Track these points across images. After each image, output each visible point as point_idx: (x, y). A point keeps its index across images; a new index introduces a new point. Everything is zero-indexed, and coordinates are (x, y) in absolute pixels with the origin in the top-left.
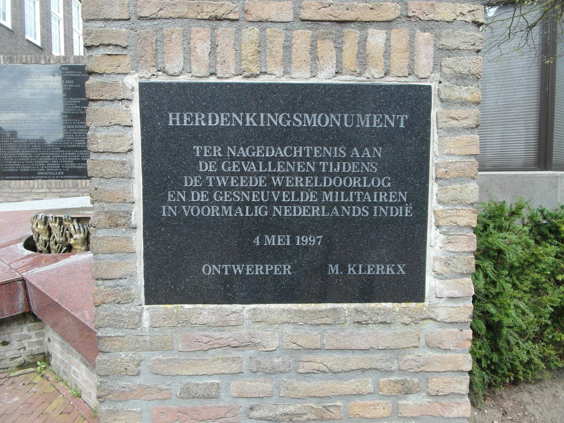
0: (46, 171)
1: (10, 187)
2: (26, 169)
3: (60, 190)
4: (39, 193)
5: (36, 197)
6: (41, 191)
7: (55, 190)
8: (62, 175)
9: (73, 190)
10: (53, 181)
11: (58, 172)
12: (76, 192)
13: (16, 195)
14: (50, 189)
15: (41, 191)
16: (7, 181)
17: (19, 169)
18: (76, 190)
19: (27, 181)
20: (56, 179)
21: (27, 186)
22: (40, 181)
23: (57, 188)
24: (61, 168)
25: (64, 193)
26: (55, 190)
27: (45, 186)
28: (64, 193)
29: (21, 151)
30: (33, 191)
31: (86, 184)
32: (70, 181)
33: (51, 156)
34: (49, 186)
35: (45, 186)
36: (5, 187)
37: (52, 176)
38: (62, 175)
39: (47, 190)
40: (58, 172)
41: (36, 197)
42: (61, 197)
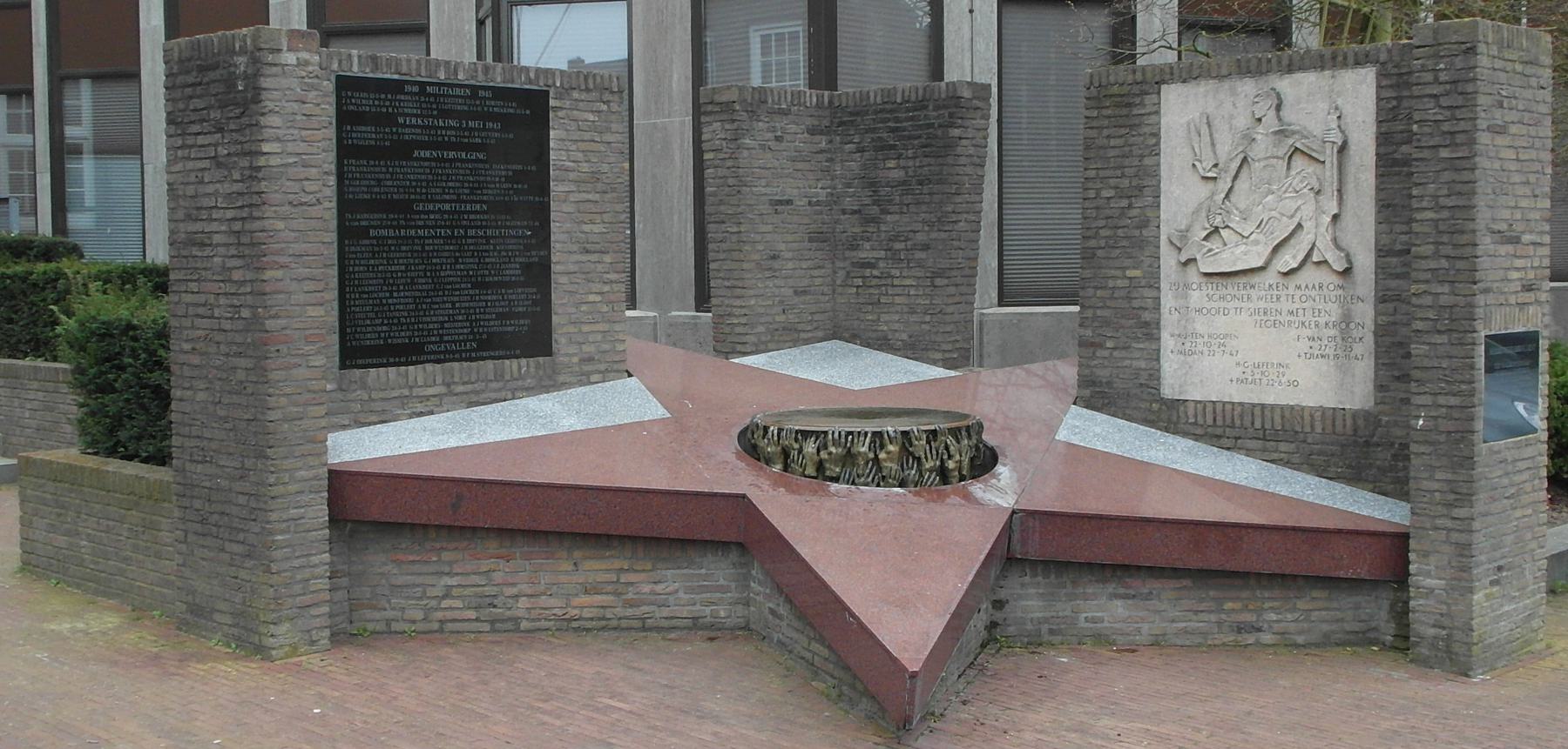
0: (441, 342)
1: (364, 386)
2: (402, 337)
3: (470, 387)
4: (428, 398)
5: (420, 408)
6: (430, 391)
7: (460, 389)
8: (474, 350)
9: (494, 385)
10: (456, 364)
11: (465, 341)
12: (500, 390)
13: (378, 406)
14: (448, 385)
15: (430, 391)
16: (358, 372)
17: (385, 339)
18: (501, 384)
19: (403, 368)
20: (460, 360)
21: (402, 381)
22: (429, 367)
23: (464, 383)
24: (472, 332)
25: (477, 392)
26: (460, 389)
27: (439, 380)
28: (477, 392)
29: (391, 292)
30: (416, 392)
31: (520, 368)
32: (490, 364)
33: (453, 303)
34: (448, 379)
35: (439, 380)
36: (354, 386)
37: (453, 352)
38: (474, 350)
39: (443, 390)
40: (465, 341)
41: (420, 408)
42: (471, 404)
